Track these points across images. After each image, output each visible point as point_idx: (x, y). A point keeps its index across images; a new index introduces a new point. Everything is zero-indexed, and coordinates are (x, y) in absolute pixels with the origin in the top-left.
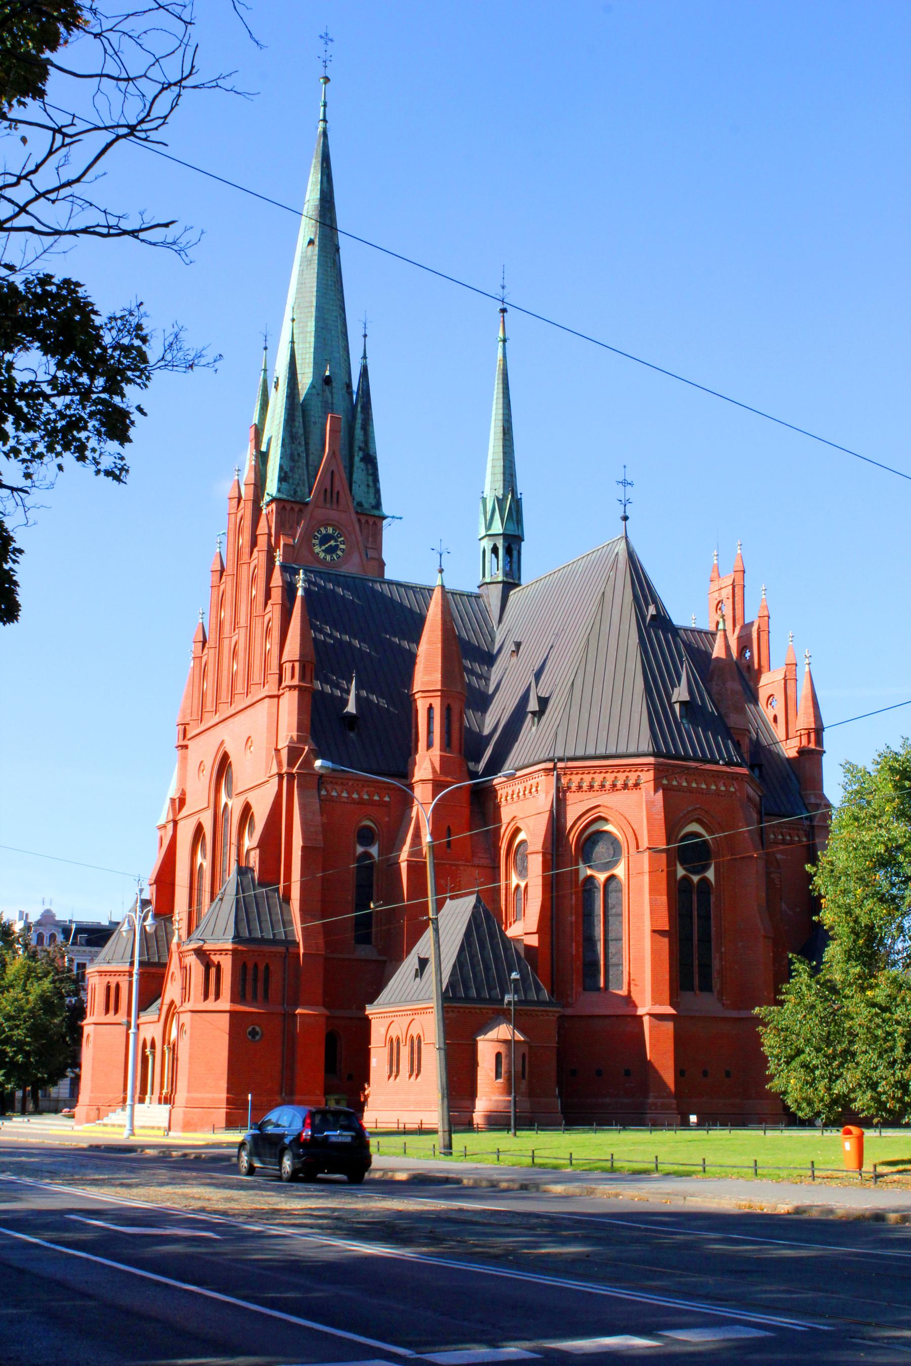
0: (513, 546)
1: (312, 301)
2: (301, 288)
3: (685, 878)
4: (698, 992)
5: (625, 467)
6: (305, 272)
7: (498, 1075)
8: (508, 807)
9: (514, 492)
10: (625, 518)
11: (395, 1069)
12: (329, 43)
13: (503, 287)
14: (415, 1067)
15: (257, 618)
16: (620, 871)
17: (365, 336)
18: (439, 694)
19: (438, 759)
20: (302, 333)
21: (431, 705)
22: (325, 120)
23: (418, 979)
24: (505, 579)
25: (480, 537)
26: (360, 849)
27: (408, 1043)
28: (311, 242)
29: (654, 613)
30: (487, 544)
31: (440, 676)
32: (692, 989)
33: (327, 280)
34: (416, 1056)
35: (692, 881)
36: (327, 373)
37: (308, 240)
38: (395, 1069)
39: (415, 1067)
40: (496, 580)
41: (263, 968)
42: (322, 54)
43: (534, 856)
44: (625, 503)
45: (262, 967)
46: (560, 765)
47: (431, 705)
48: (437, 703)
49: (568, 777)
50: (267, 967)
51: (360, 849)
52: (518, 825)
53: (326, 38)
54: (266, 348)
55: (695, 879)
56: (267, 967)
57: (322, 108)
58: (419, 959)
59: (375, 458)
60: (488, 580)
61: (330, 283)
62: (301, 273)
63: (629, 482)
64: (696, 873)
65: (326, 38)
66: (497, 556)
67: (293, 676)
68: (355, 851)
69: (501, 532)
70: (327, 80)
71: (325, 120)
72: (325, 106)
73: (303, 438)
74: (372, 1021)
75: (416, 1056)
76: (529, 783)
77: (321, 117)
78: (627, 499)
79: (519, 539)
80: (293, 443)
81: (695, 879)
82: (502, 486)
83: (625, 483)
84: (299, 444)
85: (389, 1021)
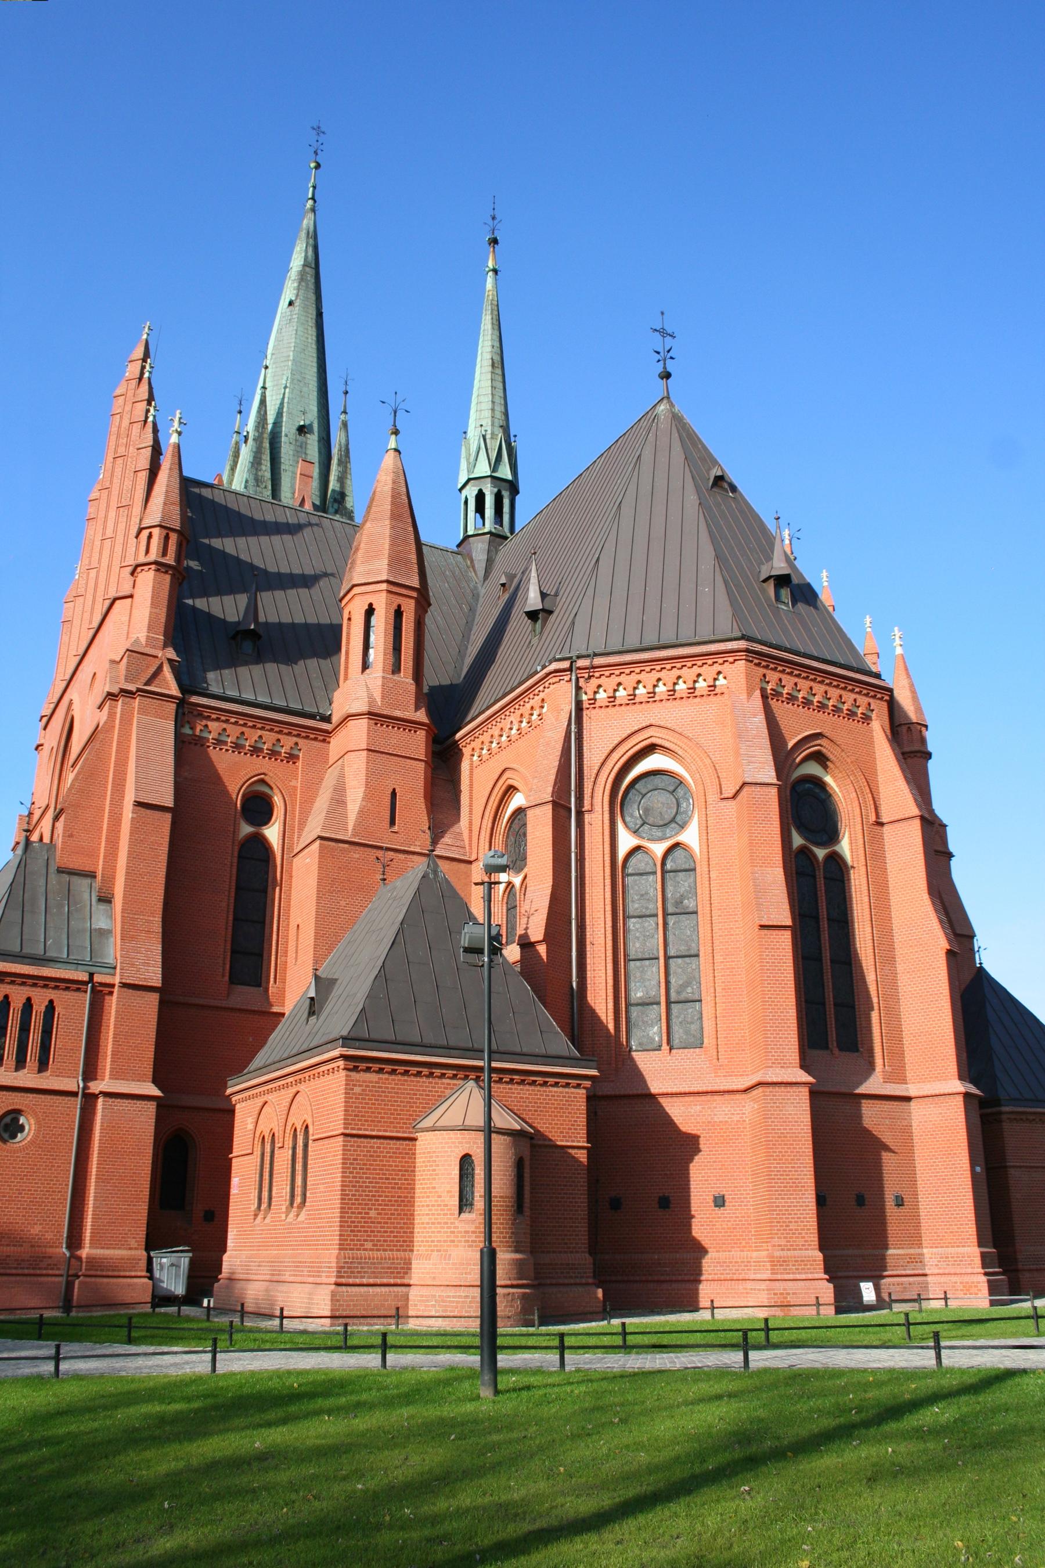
0: (506, 494)
1: (289, 356)
2: (279, 345)
3: (803, 851)
4: (836, 1051)
5: (662, 313)
6: (283, 330)
7: (464, 1203)
8: (493, 759)
9: (506, 429)
10: (666, 375)
11: (265, 1194)
12: (322, 134)
13: (494, 218)
14: (298, 1191)
15: (121, 509)
16: (691, 836)
17: (346, 393)
18: (384, 586)
19: (379, 682)
20: (277, 385)
21: (371, 605)
22: (313, 198)
23: (313, 1019)
24: (493, 530)
25: (459, 486)
26: (246, 829)
27: (289, 1143)
28: (291, 303)
29: (719, 473)
30: (471, 492)
31: (386, 562)
32: (826, 1047)
33: (307, 338)
34: (299, 1167)
35: (815, 856)
36: (302, 423)
37: (287, 303)
38: (265, 1194)
39: (298, 1191)
40: (480, 532)
41: (43, 1008)
42: (315, 144)
43: (537, 811)
44: (665, 356)
45: (39, 1007)
46: (581, 663)
47: (371, 605)
48: (382, 604)
49: (594, 682)
50: (51, 1007)
51: (246, 829)
52: (510, 782)
53: (318, 130)
54: (240, 412)
55: (821, 853)
56: (51, 1007)
57: (311, 189)
58: (317, 978)
59: (352, 512)
60: (470, 533)
61: (310, 341)
62: (279, 332)
63: (670, 331)
64: (821, 844)
65: (318, 130)
66: (483, 517)
67: (147, 551)
68: (236, 830)
69: (489, 473)
70: (318, 166)
71: (313, 198)
72: (314, 187)
73: (270, 482)
74: (238, 1106)
75: (299, 1167)
76: (528, 706)
77: (310, 196)
78: (667, 349)
79: (513, 487)
80: (258, 486)
81: (821, 853)
82: (490, 424)
83: (663, 333)
84: (265, 487)
85: (262, 1100)
